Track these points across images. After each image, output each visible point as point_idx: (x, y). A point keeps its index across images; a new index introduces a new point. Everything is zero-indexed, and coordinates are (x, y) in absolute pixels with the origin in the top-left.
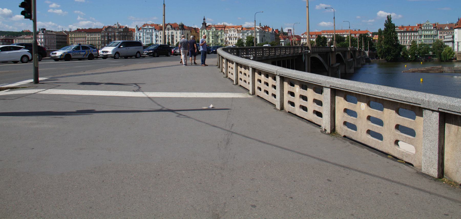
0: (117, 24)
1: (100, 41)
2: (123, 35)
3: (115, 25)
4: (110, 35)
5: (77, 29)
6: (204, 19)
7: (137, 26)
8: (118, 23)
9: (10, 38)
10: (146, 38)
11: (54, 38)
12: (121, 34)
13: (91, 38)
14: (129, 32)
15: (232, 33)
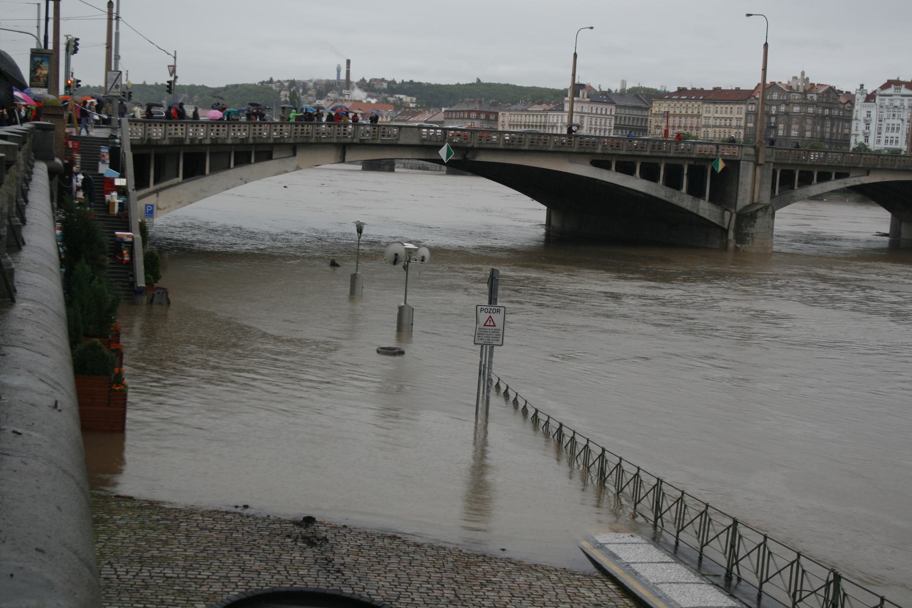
0: (799, 76)
1: (742, 131)
2: (815, 116)
3: (795, 78)
4: (774, 112)
5: (679, 88)
7: (862, 86)
8: (803, 73)
9: (492, 110)
10: (888, 129)
11: (608, 113)
12: (810, 110)
13: (716, 118)
14: (842, 106)
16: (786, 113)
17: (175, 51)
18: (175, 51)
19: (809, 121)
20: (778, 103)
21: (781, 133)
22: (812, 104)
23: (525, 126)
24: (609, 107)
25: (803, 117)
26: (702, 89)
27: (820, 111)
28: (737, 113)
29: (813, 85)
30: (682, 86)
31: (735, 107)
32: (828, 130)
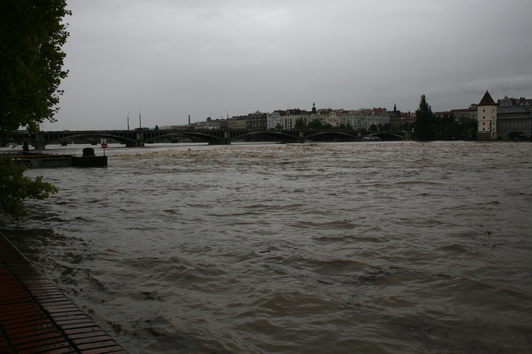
2: (261, 121)
6: (314, 104)
8: (258, 111)
12: (259, 120)
15: (333, 116)
16: (254, 121)
17: (189, 116)
18: (189, 116)
19: (259, 122)
20: (252, 118)
21: (253, 126)
22: (259, 118)
24: (218, 123)
25: (257, 121)
27: (262, 120)
28: (243, 122)
31: (244, 120)
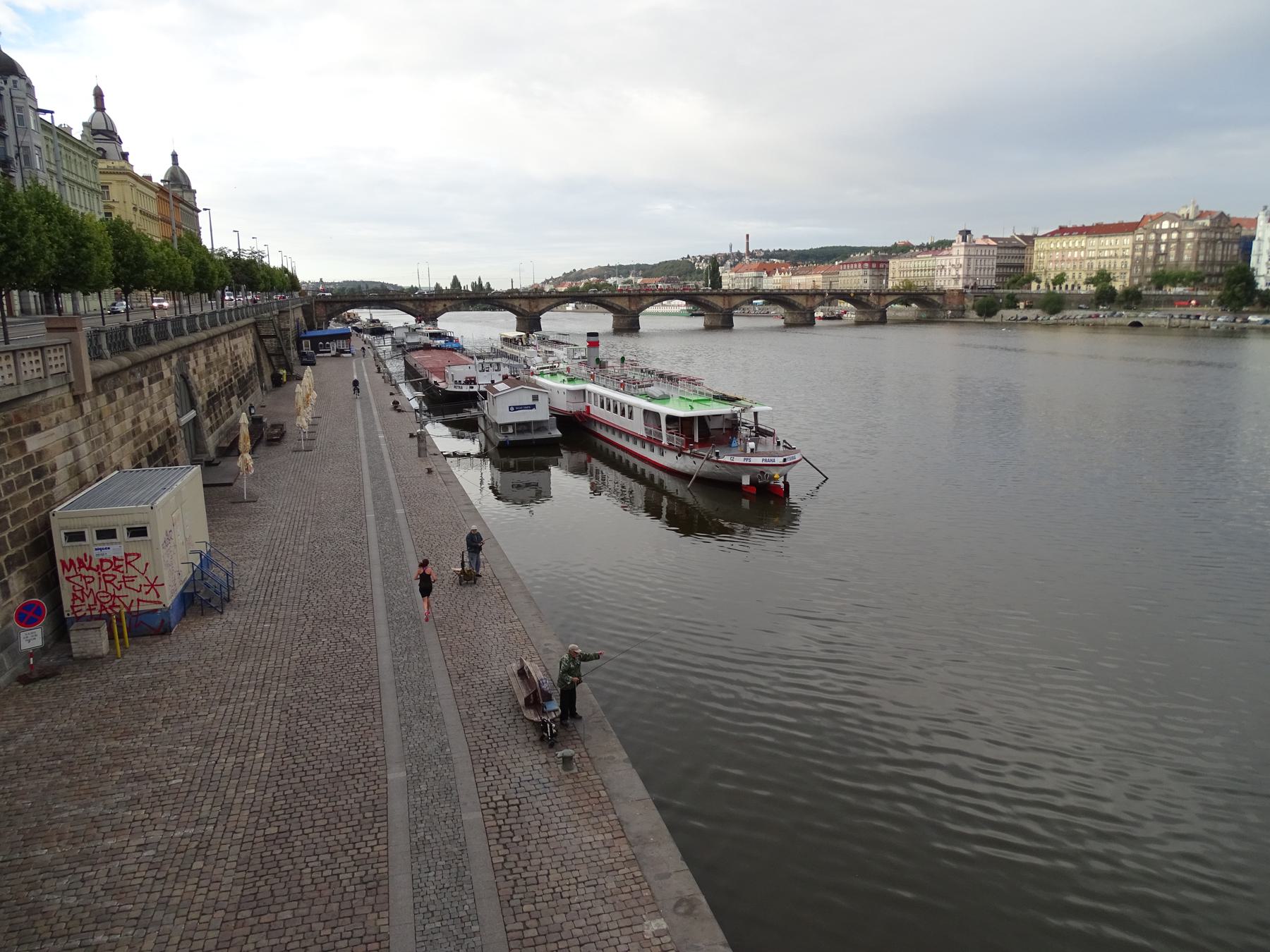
1: (1129, 261)
11: (991, 254)
21: (1172, 259)
23: (914, 271)
26: (1084, 226)
29: (1202, 212)
30: (1063, 224)
32: (1220, 252)
